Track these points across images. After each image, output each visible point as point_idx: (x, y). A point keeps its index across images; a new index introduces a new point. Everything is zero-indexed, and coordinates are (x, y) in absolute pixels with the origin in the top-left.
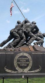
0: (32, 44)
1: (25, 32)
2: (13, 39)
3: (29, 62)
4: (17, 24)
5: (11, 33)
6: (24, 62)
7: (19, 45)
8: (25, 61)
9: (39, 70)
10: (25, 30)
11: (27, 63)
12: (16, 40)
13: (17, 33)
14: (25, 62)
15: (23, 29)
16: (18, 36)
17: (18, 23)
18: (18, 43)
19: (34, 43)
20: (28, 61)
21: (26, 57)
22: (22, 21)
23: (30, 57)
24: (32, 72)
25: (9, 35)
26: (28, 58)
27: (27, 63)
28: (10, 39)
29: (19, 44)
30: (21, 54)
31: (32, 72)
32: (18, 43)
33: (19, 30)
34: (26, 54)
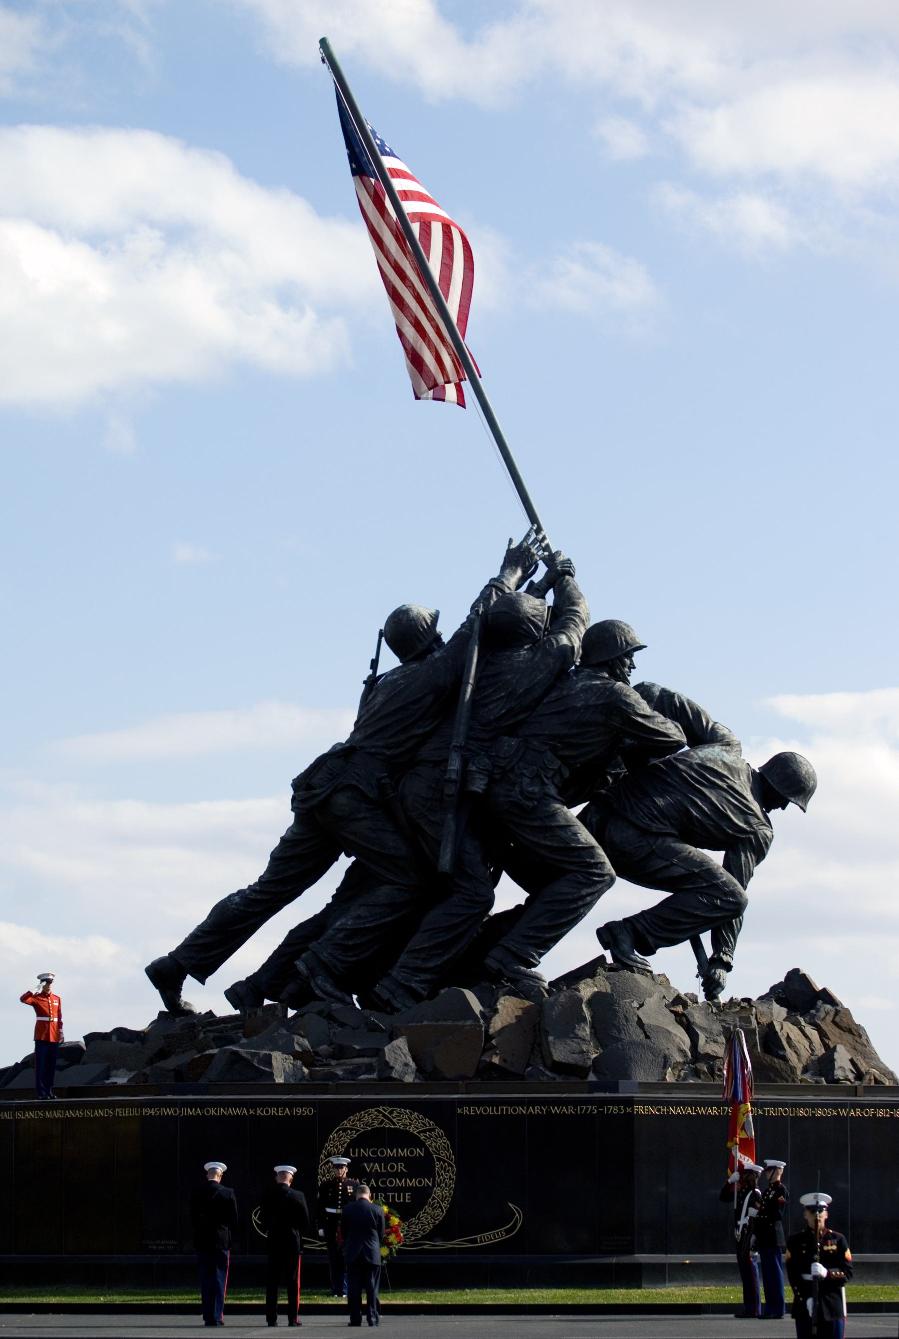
0: (575, 948)
2: (344, 862)
3: (431, 1174)
4: (390, 661)
6: (389, 1175)
7: (394, 973)
8: (400, 1167)
9: (508, 1231)
10: (479, 785)
11: (413, 1183)
14: (400, 1175)
15: (455, 764)
17: (406, 632)
19: (600, 933)
20: (423, 1166)
21: (404, 1138)
23: (438, 1142)
24: (449, 1245)
26: (421, 1144)
27: (413, 1183)
29: (403, 958)
30: (368, 1120)
31: (449, 1245)
34: (412, 1122)
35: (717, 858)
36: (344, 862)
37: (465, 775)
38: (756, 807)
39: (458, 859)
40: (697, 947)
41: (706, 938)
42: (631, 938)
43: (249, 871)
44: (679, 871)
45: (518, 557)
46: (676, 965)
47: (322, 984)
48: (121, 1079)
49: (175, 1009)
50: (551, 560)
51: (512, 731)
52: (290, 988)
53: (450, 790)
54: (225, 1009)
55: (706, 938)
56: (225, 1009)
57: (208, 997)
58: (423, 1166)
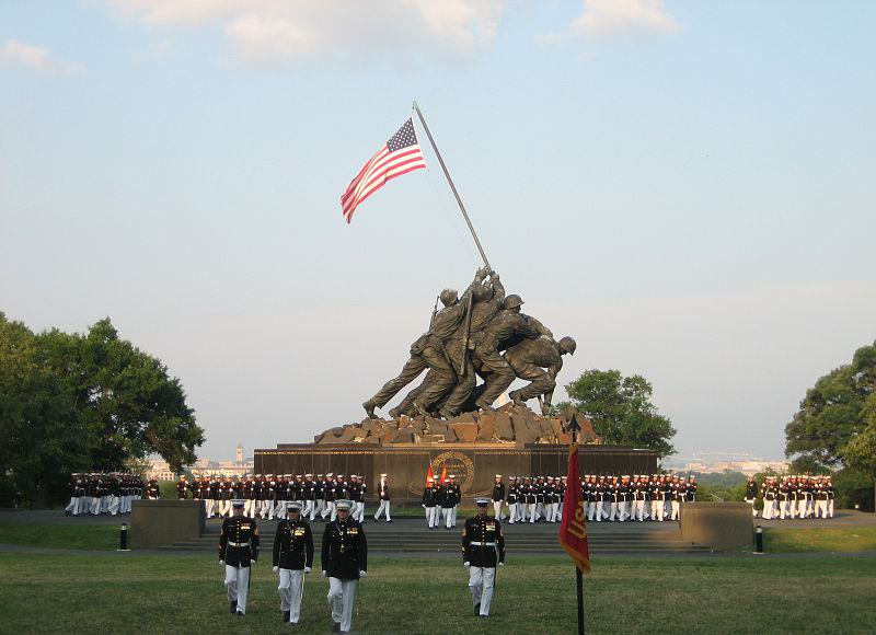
1: (470, 354)
4: (441, 306)
5: (417, 353)
10: (472, 347)
12: (434, 388)
13: (441, 354)
16: (445, 366)
18: (444, 395)
21: (459, 462)
22: (461, 287)
23: (469, 463)
25: (408, 357)
28: (409, 374)
32: (444, 395)
33: (445, 341)
34: (460, 457)
35: (546, 370)
36: (426, 371)
37: (468, 343)
38: (557, 354)
39: (466, 370)
40: (539, 398)
41: (542, 396)
42: (522, 396)
43: (396, 372)
44: (535, 375)
45: (482, 275)
46: (534, 404)
47: (421, 411)
48: (359, 440)
49: (373, 416)
50: (492, 274)
51: (482, 330)
52: (411, 412)
53: (464, 348)
54: (388, 418)
55: (542, 396)
56: (388, 418)
57: (383, 413)
58: (463, 471)
